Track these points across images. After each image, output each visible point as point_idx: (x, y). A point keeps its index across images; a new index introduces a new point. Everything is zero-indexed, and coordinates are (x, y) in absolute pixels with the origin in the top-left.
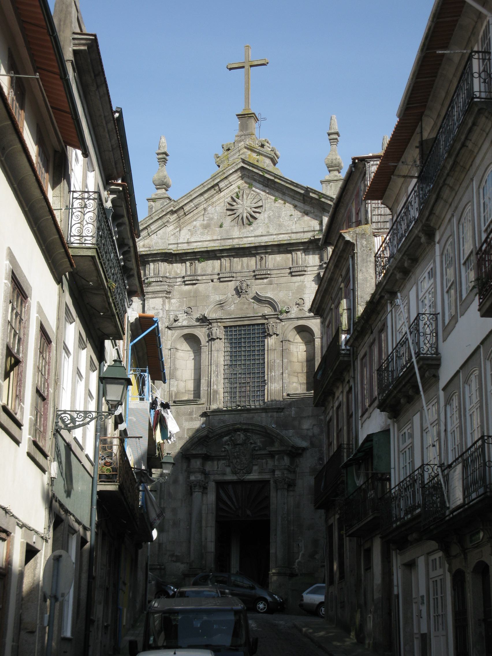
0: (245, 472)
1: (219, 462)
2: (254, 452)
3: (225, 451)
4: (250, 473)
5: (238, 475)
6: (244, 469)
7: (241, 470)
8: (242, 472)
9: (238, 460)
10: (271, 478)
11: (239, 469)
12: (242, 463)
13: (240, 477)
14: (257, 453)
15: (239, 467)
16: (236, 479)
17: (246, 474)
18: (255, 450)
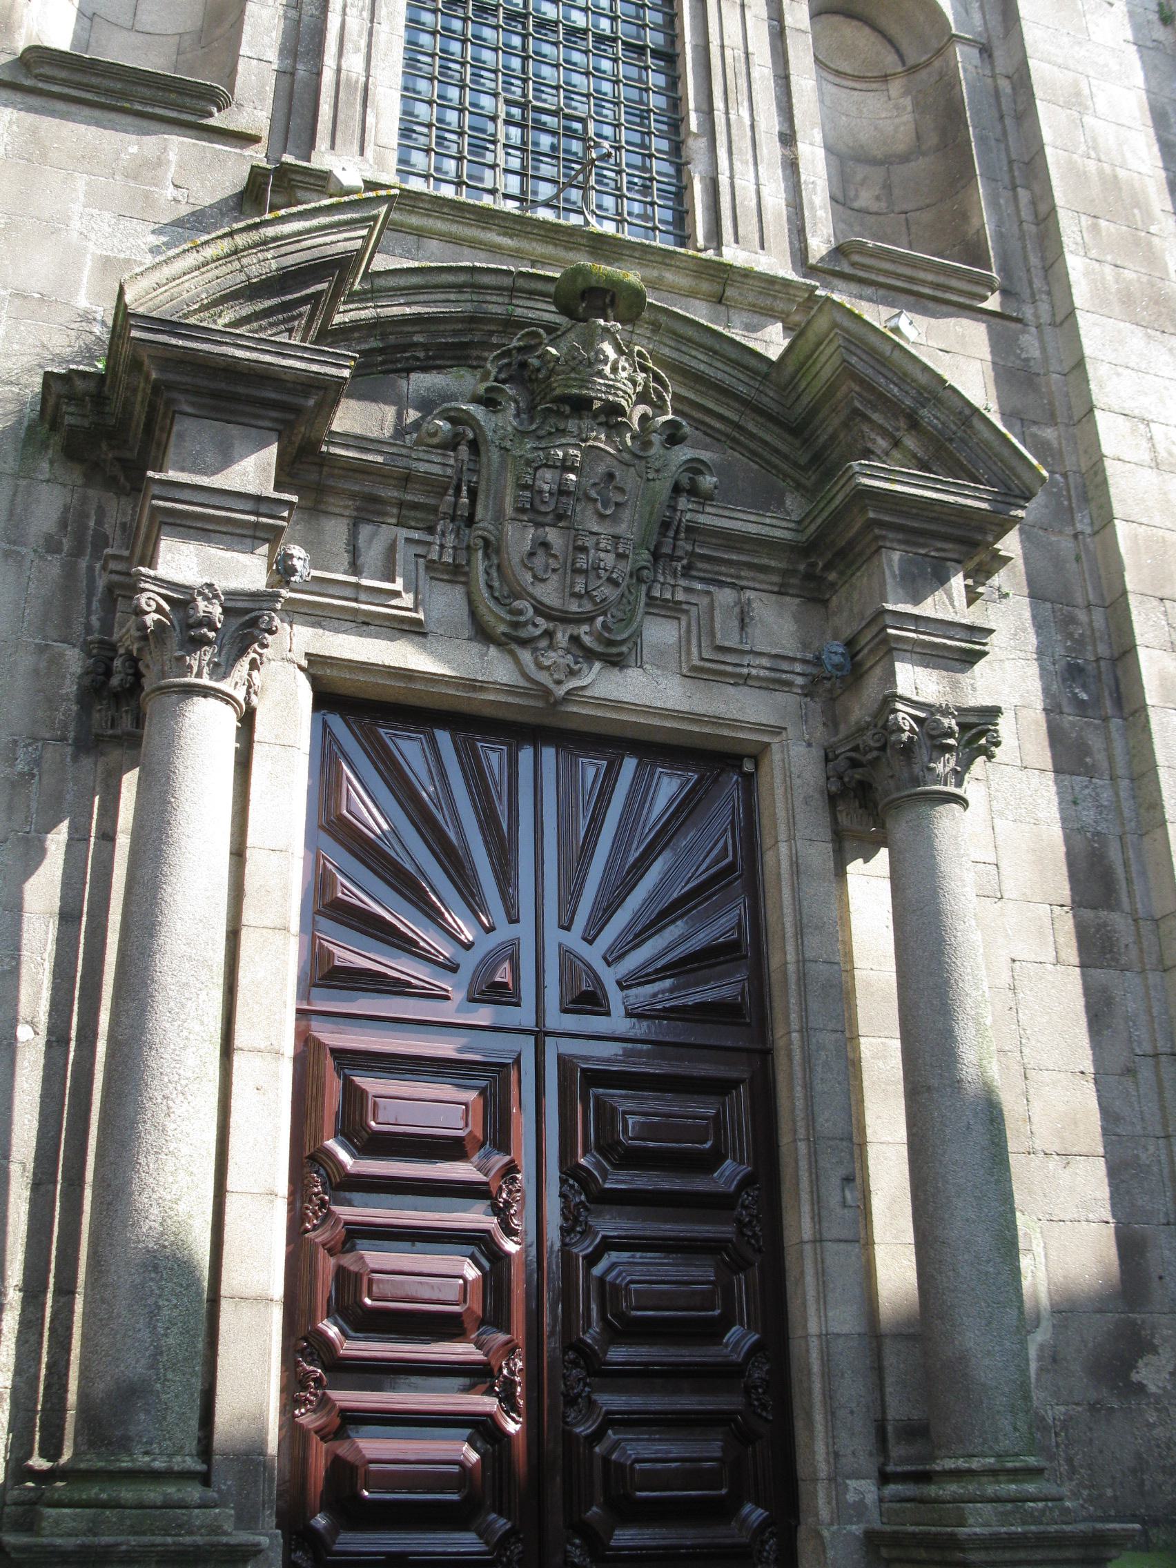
0: (587, 640)
1: (365, 530)
2: (683, 503)
3: (451, 444)
4: (616, 662)
5: (526, 656)
6: (590, 620)
7: (566, 619)
8: (562, 637)
9: (553, 535)
10: (778, 730)
11: (541, 610)
12: (582, 563)
13: (543, 677)
14: (702, 519)
15: (549, 593)
16: (510, 689)
17: (590, 655)
18: (694, 491)
